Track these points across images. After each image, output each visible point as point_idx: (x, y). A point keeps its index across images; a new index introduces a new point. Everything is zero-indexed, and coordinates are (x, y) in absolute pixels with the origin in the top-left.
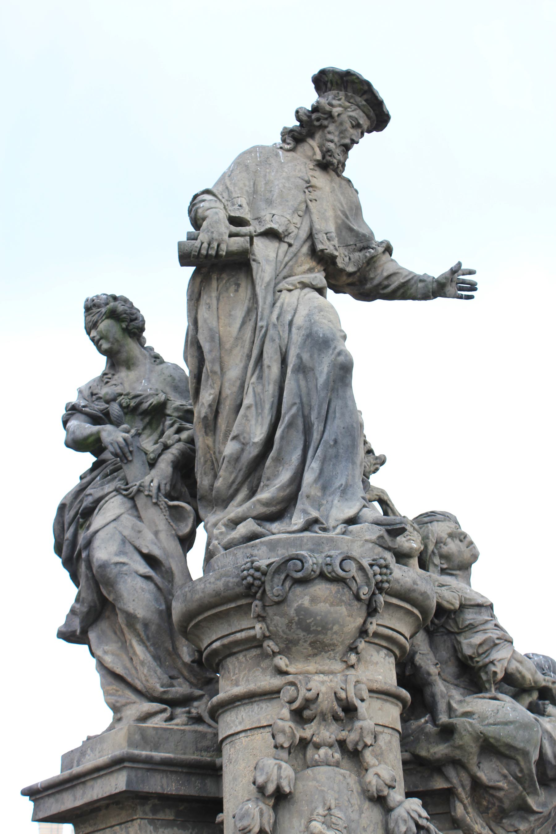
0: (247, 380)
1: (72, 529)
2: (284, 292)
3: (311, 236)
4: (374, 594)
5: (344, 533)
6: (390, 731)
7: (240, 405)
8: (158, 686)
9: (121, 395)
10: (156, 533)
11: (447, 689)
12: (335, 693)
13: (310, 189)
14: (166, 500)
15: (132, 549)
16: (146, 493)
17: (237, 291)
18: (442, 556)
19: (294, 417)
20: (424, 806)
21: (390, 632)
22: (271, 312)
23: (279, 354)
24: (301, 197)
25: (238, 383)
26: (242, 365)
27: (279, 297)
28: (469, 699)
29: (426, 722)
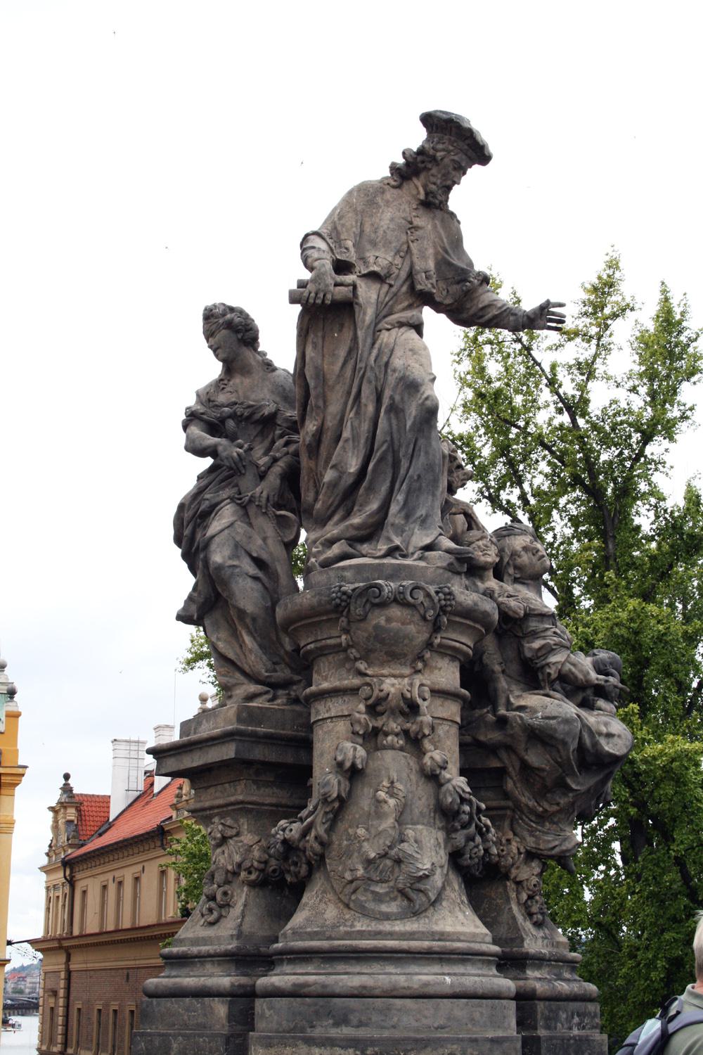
0: (347, 414)
1: (190, 527)
2: (384, 331)
3: (411, 276)
4: (439, 615)
5: (420, 559)
6: (450, 723)
7: (340, 436)
8: (263, 671)
10: (264, 539)
11: (508, 683)
12: (402, 694)
13: (413, 230)
15: (243, 552)
16: (257, 503)
17: (340, 331)
18: (516, 567)
19: (385, 452)
20: (469, 784)
22: (370, 353)
23: (375, 394)
24: (404, 238)
25: (338, 417)
26: (342, 401)
27: (379, 336)
28: (525, 695)
29: (488, 712)
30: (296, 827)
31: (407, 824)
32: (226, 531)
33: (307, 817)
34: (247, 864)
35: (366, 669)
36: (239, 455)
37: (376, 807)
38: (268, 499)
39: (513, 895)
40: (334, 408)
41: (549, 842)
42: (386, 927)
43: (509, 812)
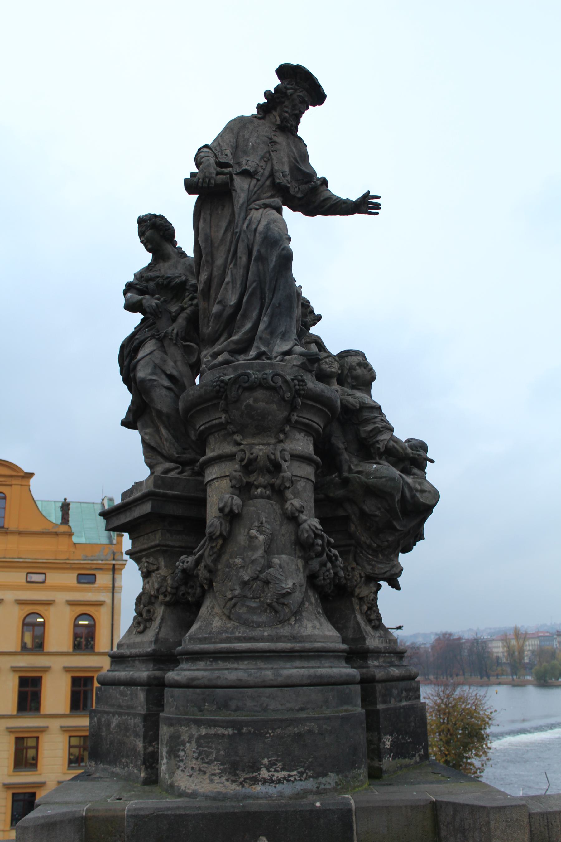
1: (128, 360)
2: (253, 210)
3: (272, 174)
5: (282, 361)
6: (305, 480)
8: (175, 453)
9: (158, 277)
10: (175, 362)
12: (268, 456)
13: (273, 144)
14: (182, 341)
16: (170, 337)
17: (223, 210)
19: (254, 289)
20: (321, 523)
21: (307, 421)
22: (243, 223)
26: (224, 257)
27: (250, 213)
28: (362, 464)
29: (336, 477)
30: (191, 559)
31: (274, 554)
32: (148, 357)
33: (198, 551)
34: (163, 589)
35: (241, 440)
36: (156, 304)
37: (250, 542)
38: (177, 334)
39: (357, 607)
40: (219, 262)
41: (382, 568)
42: (257, 633)
43: (352, 548)
